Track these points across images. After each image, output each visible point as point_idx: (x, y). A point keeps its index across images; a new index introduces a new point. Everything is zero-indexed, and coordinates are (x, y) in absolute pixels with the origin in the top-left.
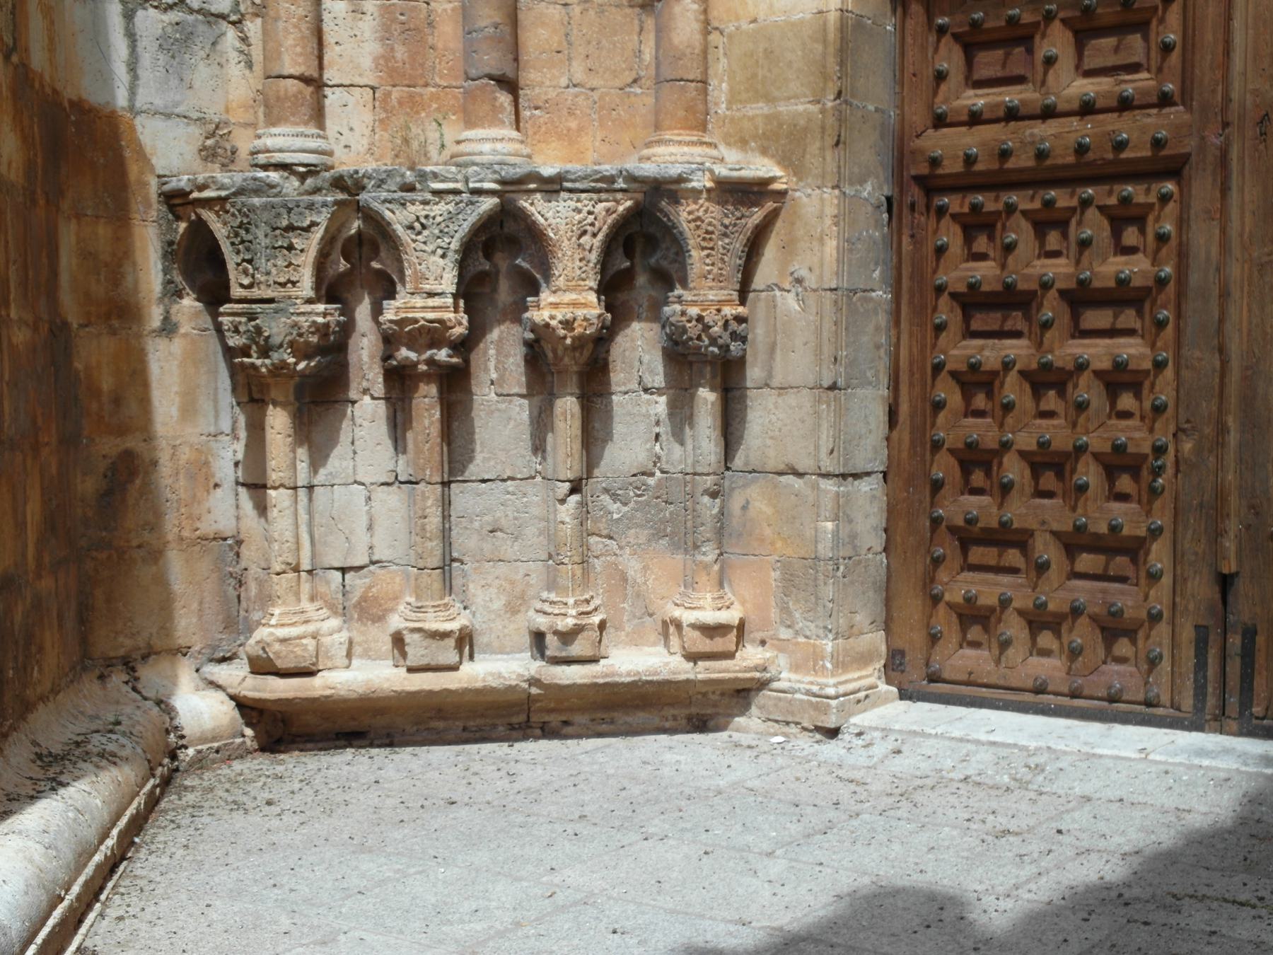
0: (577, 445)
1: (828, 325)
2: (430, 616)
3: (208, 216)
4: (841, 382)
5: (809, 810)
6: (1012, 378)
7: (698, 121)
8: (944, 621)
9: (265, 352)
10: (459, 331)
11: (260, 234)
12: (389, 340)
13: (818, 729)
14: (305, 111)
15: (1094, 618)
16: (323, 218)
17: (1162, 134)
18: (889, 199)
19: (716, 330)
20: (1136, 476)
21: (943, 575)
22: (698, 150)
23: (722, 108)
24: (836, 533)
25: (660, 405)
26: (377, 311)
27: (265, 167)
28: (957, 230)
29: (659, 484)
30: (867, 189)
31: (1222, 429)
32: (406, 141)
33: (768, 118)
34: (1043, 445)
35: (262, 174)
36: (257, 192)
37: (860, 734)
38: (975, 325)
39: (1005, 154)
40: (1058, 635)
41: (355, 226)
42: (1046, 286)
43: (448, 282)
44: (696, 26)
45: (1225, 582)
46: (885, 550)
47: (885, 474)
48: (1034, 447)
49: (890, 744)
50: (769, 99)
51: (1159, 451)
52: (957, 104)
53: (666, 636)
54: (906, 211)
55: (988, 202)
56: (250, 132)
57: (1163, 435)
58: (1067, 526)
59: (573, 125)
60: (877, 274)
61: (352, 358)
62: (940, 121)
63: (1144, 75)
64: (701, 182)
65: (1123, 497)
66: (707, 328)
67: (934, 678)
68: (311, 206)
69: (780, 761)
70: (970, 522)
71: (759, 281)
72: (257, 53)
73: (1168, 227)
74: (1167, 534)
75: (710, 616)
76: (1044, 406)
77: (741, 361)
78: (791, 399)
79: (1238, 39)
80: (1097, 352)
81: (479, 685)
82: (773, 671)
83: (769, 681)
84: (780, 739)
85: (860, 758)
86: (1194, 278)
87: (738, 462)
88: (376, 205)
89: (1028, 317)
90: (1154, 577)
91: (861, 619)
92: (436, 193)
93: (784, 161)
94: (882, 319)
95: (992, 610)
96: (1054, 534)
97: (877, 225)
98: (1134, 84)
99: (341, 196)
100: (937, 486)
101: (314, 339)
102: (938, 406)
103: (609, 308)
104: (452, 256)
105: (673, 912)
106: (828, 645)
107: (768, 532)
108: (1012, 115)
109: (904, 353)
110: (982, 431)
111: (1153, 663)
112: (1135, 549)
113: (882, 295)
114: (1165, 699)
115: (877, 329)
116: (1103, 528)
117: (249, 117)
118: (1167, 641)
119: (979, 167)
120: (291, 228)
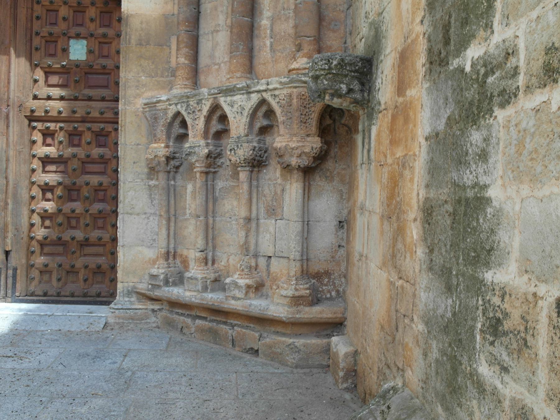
79: (12, 79)
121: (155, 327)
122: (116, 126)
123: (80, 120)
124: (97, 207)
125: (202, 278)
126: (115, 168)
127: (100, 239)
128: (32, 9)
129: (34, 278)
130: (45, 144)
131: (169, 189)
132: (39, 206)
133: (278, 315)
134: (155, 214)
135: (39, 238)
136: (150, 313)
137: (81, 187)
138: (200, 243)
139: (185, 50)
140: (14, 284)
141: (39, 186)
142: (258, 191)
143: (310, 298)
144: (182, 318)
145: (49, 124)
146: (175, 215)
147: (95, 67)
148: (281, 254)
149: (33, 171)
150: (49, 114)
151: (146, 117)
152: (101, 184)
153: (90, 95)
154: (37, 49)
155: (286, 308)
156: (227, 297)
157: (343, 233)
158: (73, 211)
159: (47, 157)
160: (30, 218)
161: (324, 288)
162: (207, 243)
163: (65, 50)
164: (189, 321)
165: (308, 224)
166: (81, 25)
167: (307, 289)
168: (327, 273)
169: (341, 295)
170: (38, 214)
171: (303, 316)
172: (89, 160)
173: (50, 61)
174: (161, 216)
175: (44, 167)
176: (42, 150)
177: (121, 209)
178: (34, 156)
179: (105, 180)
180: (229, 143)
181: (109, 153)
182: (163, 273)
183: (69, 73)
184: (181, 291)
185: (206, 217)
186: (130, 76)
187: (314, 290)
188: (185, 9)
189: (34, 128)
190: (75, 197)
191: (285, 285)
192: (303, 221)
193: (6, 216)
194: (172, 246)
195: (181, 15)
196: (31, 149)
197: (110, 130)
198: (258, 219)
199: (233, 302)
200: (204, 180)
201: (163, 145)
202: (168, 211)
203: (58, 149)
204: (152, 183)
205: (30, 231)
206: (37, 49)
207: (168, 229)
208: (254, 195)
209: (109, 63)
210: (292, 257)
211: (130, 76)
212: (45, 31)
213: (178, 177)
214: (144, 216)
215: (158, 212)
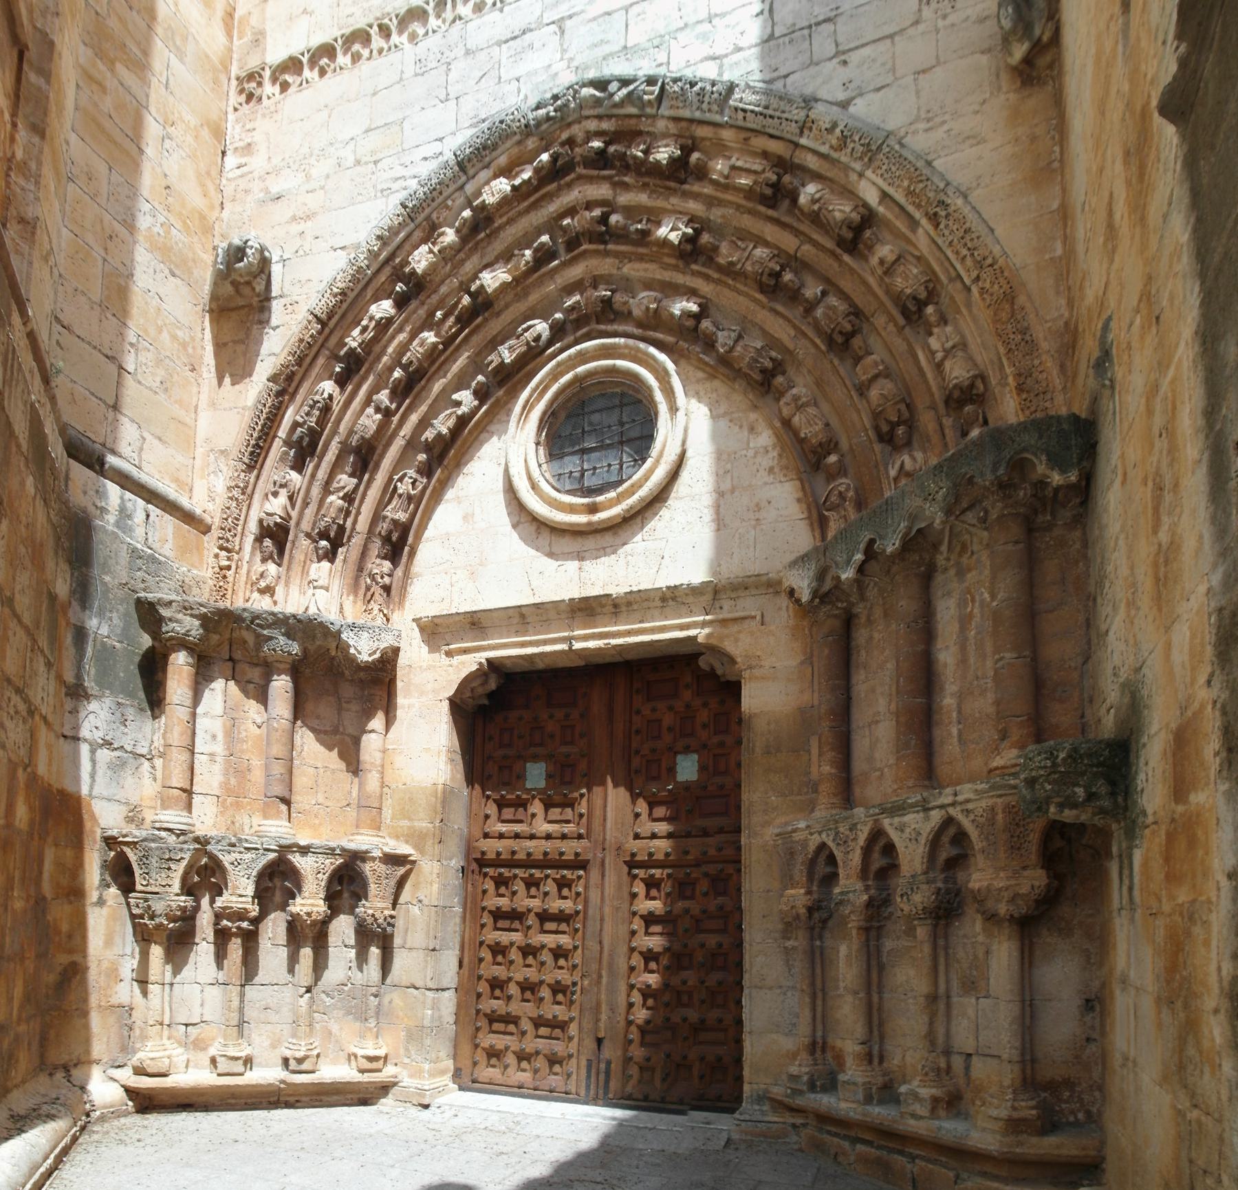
0: (311, 970)
2: (231, 1048)
3: (126, 849)
8: (480, 1056)
9: (152, 918)
10: (254, 914)
11: (154, 861)
12: (218, 917)
14: (182, 804)
15: (545, 1056)
16: (187, 856)
19: (380, 921)
20: (565, 995)
21: (480, 1035)
25: (352, 953)
26: (212, 902)
27: (159, 829)
29: (350, 990)
31: (600, 976)
32: (233, 823)
33: (409, 828)
35: (157, 832)
36: (153, 841)
40: (529, 1063)
41: (204, 860)
42: (529, 911)
43: (250, 891)
44: (378, 784)
45: (599, 1041)
49: (453, 1112)
51: (575, 984)
53: (349, 1060)
56: (152, 811)
57: (577, 978)
58: (535, 1015)
59: (317, 822)
61: (198, 923)
64: (377, 853)
65: (559, 1003)
66: (376, 920)
67: (474, 1082)
68: (181, 850)
69: (401, 1120)
71: (402, 900)
72: (159, 774)
74: (577, 1020)
75: (372, 1052)
77: (392, 936)
81: (254, 1083)
82: (400, 1078)
87: (388, 981)
88: (215, 852)
89: (521, 923)
90: (571, 1039)
91: (443, 1054)
92: (246, 848)
95: (501, 1051)
96: (531, 1019)
99: (197, 846)
101: (179, 913)
102: (481, 960)
103: (329, 908)
104: (253, 879)
106: (427, 1066)
109: (467, 936)
111: (569, 1076)
112: (563, 1026)
113: (458, 909)
114: (574, 1091)
116: (550, 1017)
117: (153, 804)
118: (575, 1066)
120: (170, 859)
124: (714, 978)
125: (864, 1084)
129: (631, 1076)
130: (648, 897)
131: (813, 952)
133: (984, 1147)
134: (794, 988)
135: (640, 1022)
138: (859, 1030)
139: (830, 755)
140: (607, 1082)
142: (947, 954)
143: (1039, 1123)
146: (823, 990)
148: (987, 1051)
149: (633, 933)
155: (998, 1137)
156: (902, 1115)
157: (1093, 1018)
160: (629, 995)
161: (1064, 1106)
162: (871, 1031)
165: (1031, 1005)
167: (1032, 1108)
168: (1069, 1083)
169: (1093, 1120)
170: (639, 990)
171: (1026, 1151)
174: (803, 991)
177: (746, 982)
178: (634, 914)
180: (900, 883)
185: (869, 993)
187: (1042, 1106)
188: (829, 696)
191: (995, 1101)
192: (1023, 1001)
193: (599, 992)
194: (819, 1034)
196: (631, 904)
197: (731, 871)
198: (948, 997)
199: (912, 1122)
200: (863, 938)
201: (802, 891)
203: (665, 904)
205: (628, 1013)
207: (814, 1009)
208: (942, 960)
210: (1005, 1056)
213: (827, 934)
215: (798, 986)
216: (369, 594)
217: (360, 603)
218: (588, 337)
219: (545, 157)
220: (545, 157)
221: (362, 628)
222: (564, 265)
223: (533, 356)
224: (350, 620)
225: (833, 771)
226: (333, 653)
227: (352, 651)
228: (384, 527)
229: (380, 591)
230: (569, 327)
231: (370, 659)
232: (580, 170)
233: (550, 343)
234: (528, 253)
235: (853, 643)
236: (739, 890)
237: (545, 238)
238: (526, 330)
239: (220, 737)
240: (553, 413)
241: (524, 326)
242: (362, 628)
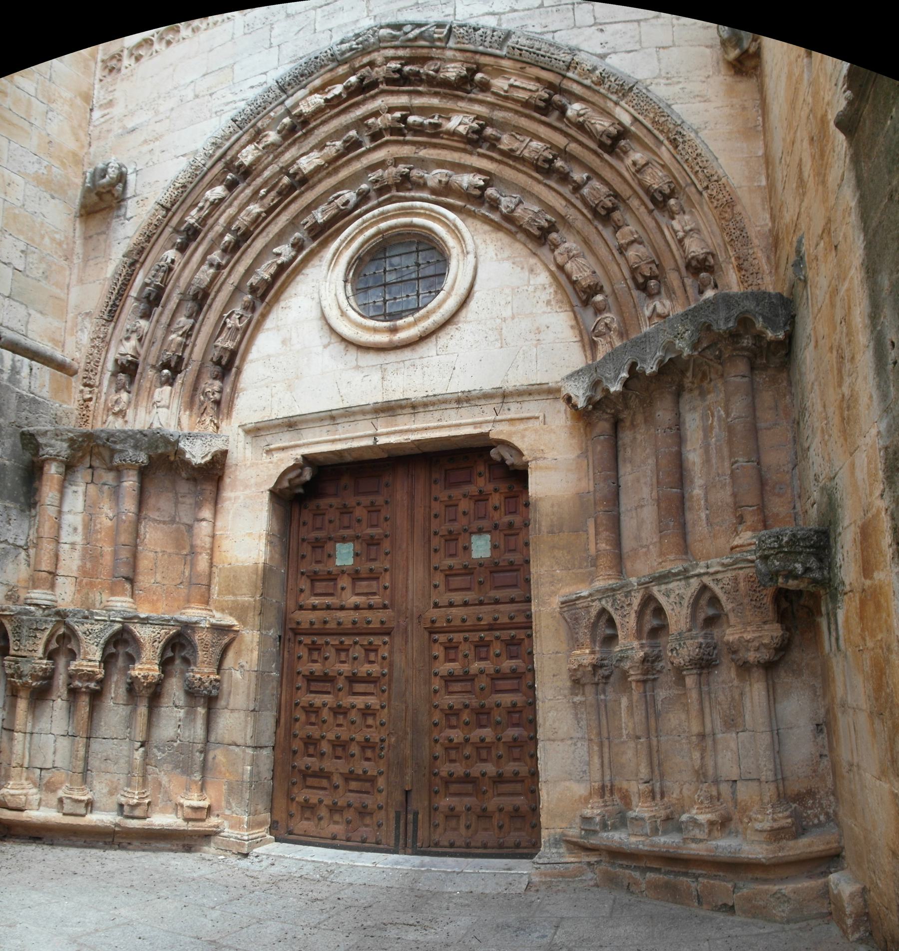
1: (253, 686)
4: (257, 709)
5: (232, 889)
6: (326, 710)
7: (206, 601)
13: (239, 853)
17: (384, 619)
18: (280, 637)
22: (204, 612)
23: (215, 597)
24: (251, 771)
28: (306, 650)
30: (271, 632)
34: (338, 738)
37: (257, 857)
38: (312, 689)
39: (325, 622)
42: (340, 674)
46: (272, 779)
47: (274, 747)
48: (334, 738)
50: (234, 594)
52: (308, 602)
54: (286, 642)
55: (320, 640)
60: (274, 666)
62: (301, 608)
63: (377, 597)
70: (308, 768)
72: (32, 561)
73: (386, 654)
76: (338, 722)
78: (236, 714)
80: (360, 702)
83: (220, 832)
84: (223, 857)
85: (256, 867)
86: (395, 675)
93: (239, 619)
94: (275, 684)
97: (275, 646)
98: (375, 600)
100: (295, 752)
105: (167, 931)
107: (223, 769)
108: (328, 608)
110: (314, 731)
115: (273, 688)
119: (315, 626)
121: (592, 886)
122: (529, 633)
123: (487, 627)
124: (512, 733)
126: (530, 683)
127: (516, 774)
128: (430, 507)
132: (443, 734)
136: (585, 867)
137: (491, 709)
139: (605, 534)
141: (442, 710)
144: (627, 871)
145: (451, 636)
147: (501, 564)
150: (452, 624)
151: (564, 618)
152: (514, 705)
153: (497, 597)
154: (436, 551)
158: (482, 740)
159: (451, 674)
163: (467, 549)
164: (637, 875)
166: (484, 518)
170: (442, 745)
172: (499, 676)
173: (450, 562)
175: (447, 687)
176: (445, 668)
179: (518, 698)
181: (522, 665)
182: (598, 815)
183: (472, 573)
184: (623, 836)
186: (543, 570)
188: (602, 485)
189: (435, 641)
190: (484, 722)
195: (597, 494)
202: (599, 734)
204: (578, 699)
206: (436, 551)
209: (516, 557)
211: (543, 570)
212: (444, 529)
214: (569, 742)
216: (203, 408)
217: (194, 416)
218: (389, 201)
219: (353, 79)
220: (353, 79)
221: (196, 436)
222: (369, 151)
223: (342, 217)
224: (186, 431)
225: (608, 548)
226: (172, 458)
227: (188, 456)
228: (216, 354)
229: (210, 405)
230: (372, 194)
231: (203, 462)
232: (383, 87)
233: (357, 206)
234: (338, 143)
235: (620, 443)
236: (531, 654)
237: (353, 133)
238: (336, 198)
239: (80, 529)
240: (360, 259)
241: (335, 195)
242: (196, 436)
